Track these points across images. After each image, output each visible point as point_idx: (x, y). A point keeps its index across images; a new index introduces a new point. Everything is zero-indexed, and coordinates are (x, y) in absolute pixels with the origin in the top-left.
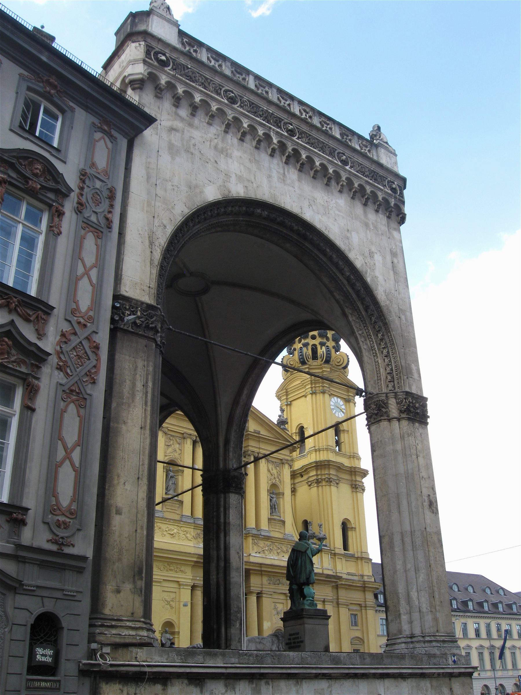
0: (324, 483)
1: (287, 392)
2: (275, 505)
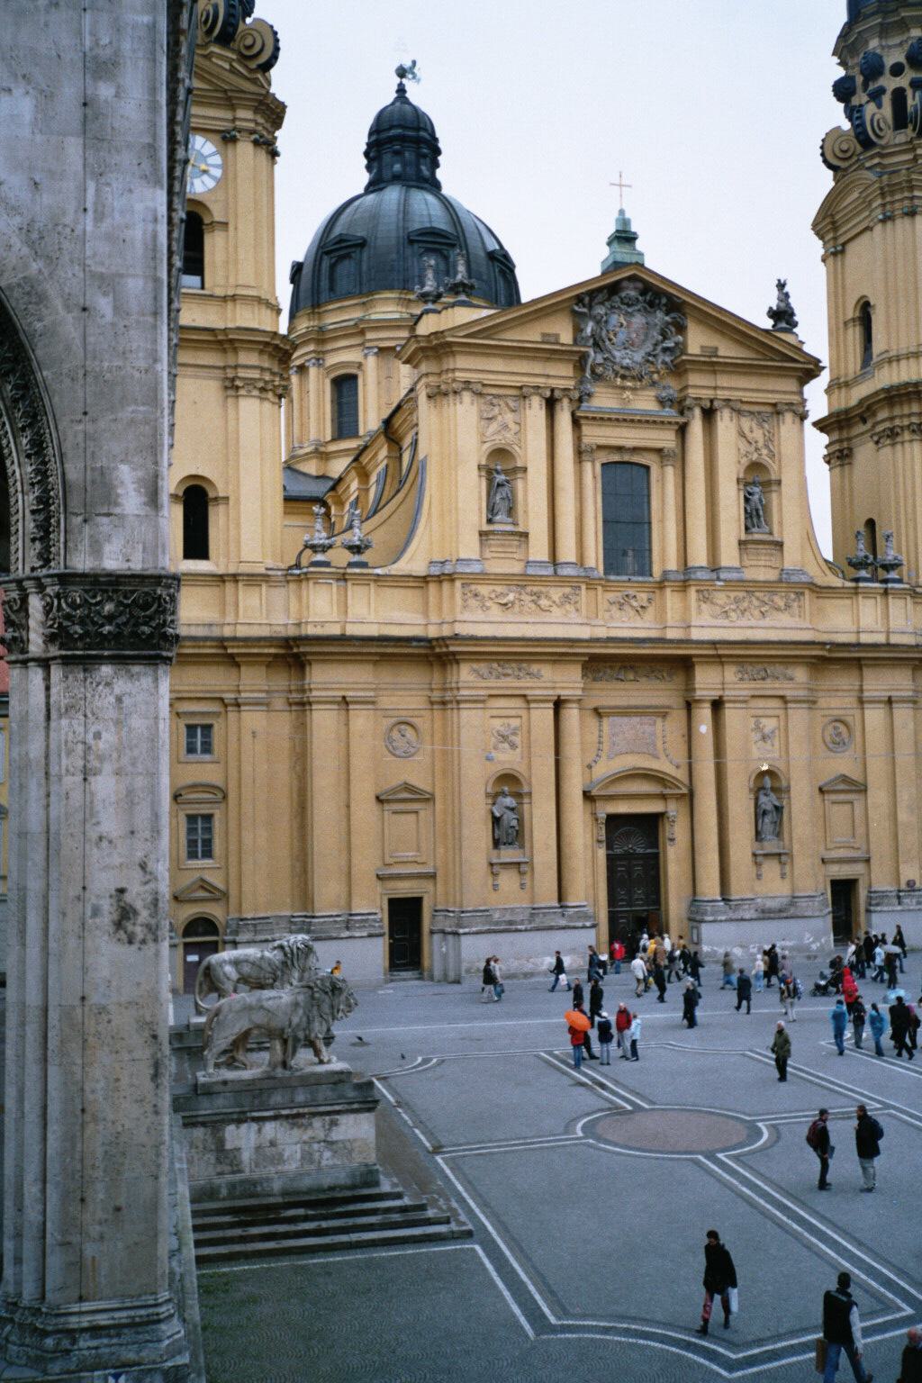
0: (907, 436)
1: (833, 223)
2: (757, 510)
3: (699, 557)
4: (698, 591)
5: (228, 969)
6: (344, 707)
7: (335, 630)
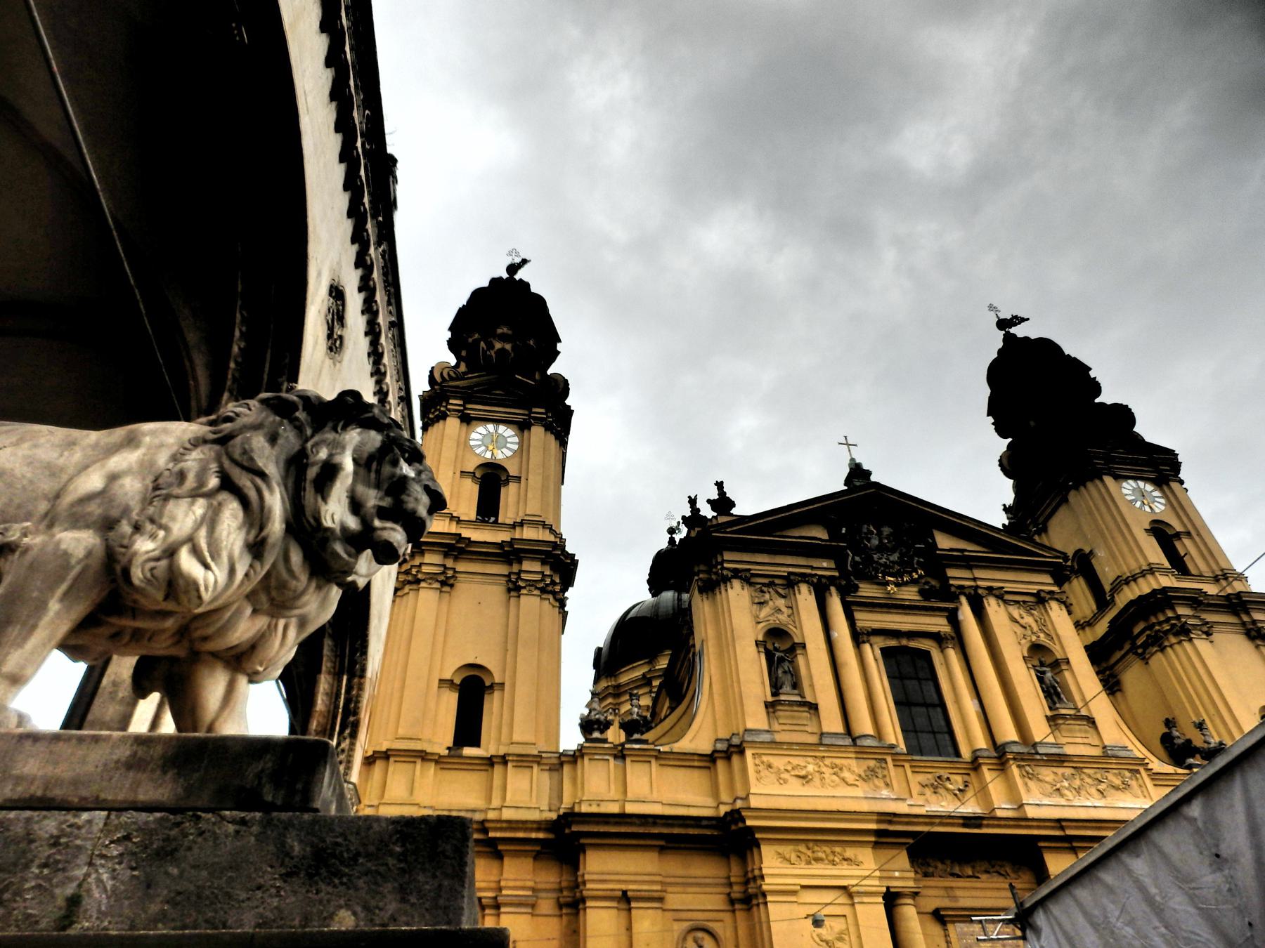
2: (1054, 688)
3: (1008, 732)
4: (1019, 766)
6: (624, 906)
7: (614, 809)
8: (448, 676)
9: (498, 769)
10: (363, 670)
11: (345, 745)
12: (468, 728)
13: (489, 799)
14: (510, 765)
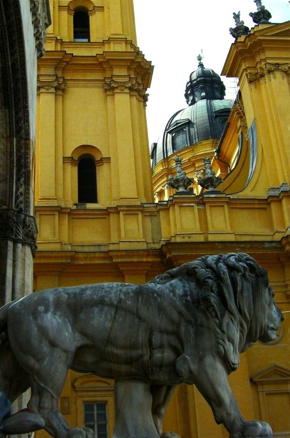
5: (52, 320)
7: (201, 239)
8: (69, 154)
9: (113, 218)
10: (28, 134)
11: (22, 190)
12: (87, 189)
13: (109, 236)
14: (121, 214)
